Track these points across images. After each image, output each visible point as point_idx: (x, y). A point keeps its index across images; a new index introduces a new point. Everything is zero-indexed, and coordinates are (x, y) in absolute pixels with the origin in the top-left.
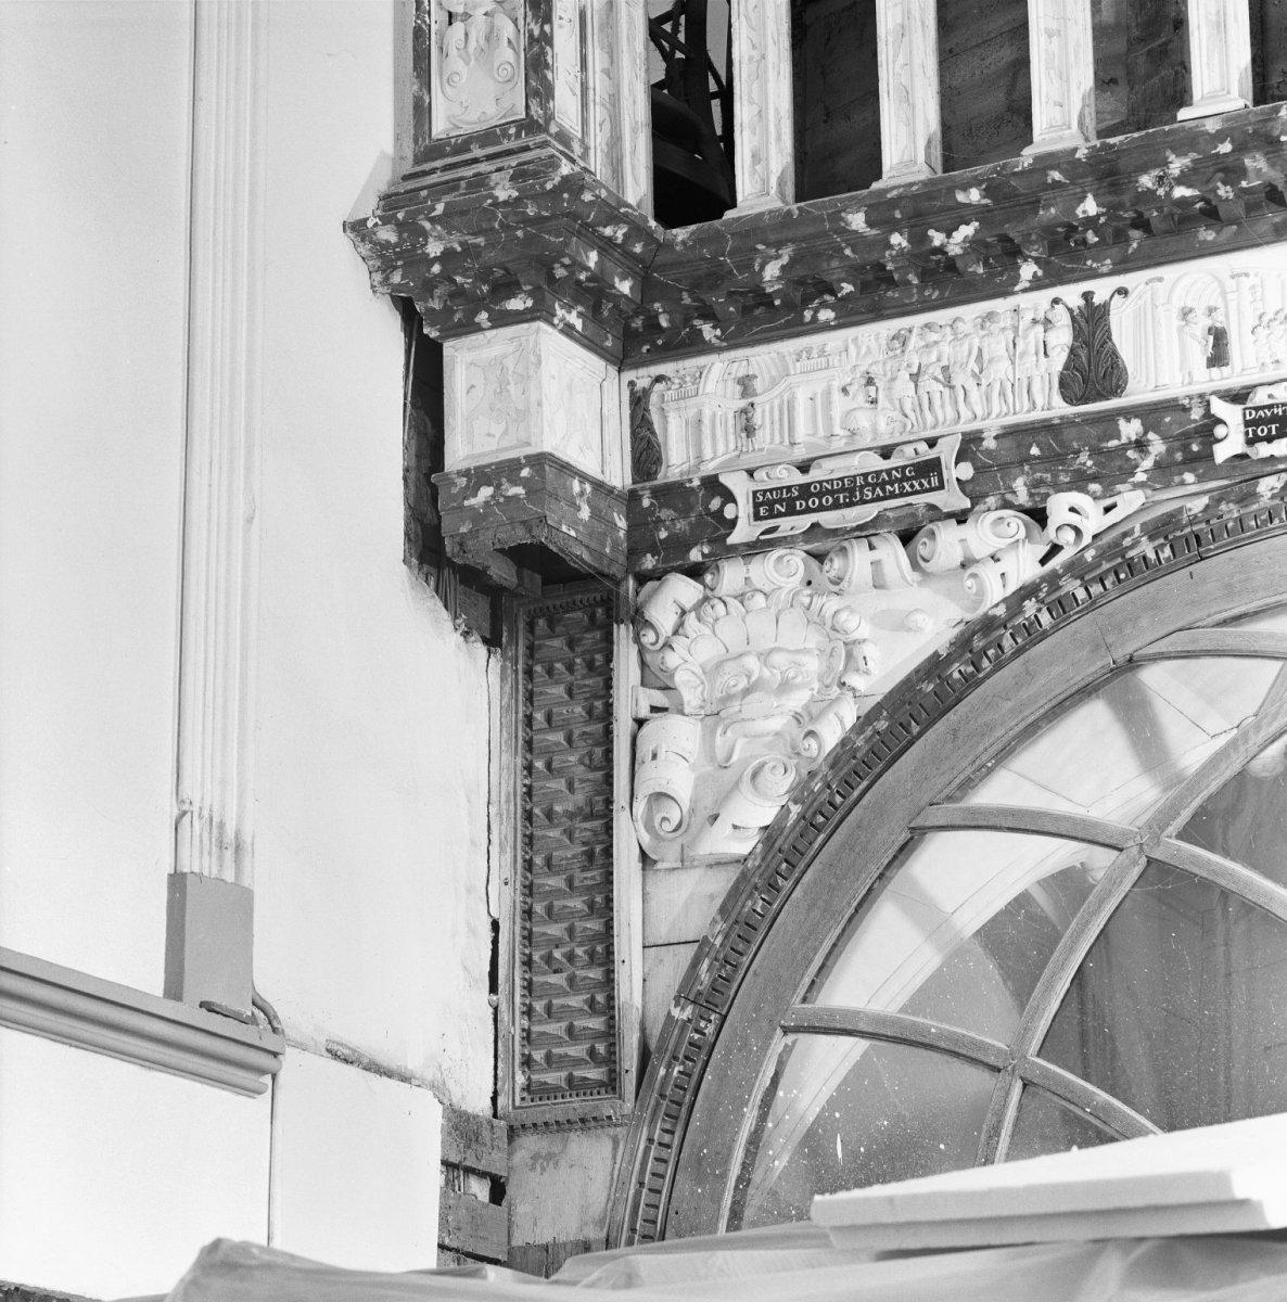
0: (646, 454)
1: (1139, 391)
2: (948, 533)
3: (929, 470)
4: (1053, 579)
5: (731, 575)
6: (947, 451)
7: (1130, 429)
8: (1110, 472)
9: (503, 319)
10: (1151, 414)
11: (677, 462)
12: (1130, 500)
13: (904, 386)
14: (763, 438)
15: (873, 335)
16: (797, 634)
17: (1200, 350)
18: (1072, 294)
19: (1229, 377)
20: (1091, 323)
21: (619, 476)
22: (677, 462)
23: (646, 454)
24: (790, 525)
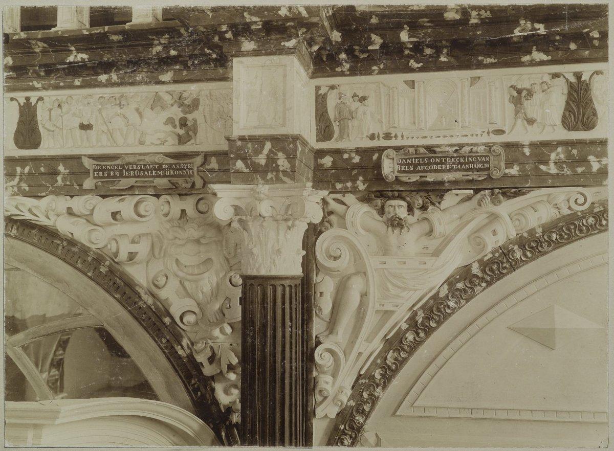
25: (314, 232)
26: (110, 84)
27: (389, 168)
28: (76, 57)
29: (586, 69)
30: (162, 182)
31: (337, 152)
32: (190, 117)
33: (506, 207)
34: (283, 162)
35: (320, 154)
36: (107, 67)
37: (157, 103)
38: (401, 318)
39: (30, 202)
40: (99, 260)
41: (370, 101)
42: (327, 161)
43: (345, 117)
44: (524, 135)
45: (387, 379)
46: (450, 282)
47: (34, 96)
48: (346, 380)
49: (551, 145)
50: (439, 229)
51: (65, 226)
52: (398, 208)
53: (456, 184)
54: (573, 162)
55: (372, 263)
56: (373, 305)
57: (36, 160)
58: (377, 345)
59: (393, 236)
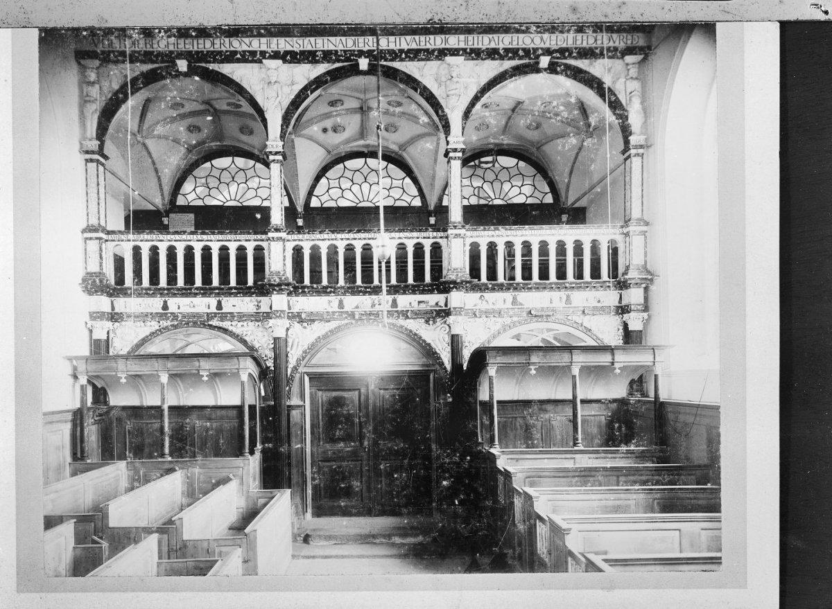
0: (113, 308)
1: (170, 311)
4: (160, 329)
5: (123, 323)
7: (170, 315)
9: (97, 295)
10: (171, 313)
12: (168, 321)
18: (163, 299)
19: (179, 311)
20: (165, 302)
21: (110, 311)
23: (113, 308)
25: (288, 329)
27: (303, 316)
28: (233, 291)
35: (289, 313)
36: (240, 293)
38: (306, 347)
39: (221, 323)
40: (238, 336)
42: (290, 315)
44: (330, 310)
45: (303, 360)
47: (221, 299)
48: (295, 360)
51: (230, 328)
52: (305, 324)
56: (300, 344)
58: (301, 352)
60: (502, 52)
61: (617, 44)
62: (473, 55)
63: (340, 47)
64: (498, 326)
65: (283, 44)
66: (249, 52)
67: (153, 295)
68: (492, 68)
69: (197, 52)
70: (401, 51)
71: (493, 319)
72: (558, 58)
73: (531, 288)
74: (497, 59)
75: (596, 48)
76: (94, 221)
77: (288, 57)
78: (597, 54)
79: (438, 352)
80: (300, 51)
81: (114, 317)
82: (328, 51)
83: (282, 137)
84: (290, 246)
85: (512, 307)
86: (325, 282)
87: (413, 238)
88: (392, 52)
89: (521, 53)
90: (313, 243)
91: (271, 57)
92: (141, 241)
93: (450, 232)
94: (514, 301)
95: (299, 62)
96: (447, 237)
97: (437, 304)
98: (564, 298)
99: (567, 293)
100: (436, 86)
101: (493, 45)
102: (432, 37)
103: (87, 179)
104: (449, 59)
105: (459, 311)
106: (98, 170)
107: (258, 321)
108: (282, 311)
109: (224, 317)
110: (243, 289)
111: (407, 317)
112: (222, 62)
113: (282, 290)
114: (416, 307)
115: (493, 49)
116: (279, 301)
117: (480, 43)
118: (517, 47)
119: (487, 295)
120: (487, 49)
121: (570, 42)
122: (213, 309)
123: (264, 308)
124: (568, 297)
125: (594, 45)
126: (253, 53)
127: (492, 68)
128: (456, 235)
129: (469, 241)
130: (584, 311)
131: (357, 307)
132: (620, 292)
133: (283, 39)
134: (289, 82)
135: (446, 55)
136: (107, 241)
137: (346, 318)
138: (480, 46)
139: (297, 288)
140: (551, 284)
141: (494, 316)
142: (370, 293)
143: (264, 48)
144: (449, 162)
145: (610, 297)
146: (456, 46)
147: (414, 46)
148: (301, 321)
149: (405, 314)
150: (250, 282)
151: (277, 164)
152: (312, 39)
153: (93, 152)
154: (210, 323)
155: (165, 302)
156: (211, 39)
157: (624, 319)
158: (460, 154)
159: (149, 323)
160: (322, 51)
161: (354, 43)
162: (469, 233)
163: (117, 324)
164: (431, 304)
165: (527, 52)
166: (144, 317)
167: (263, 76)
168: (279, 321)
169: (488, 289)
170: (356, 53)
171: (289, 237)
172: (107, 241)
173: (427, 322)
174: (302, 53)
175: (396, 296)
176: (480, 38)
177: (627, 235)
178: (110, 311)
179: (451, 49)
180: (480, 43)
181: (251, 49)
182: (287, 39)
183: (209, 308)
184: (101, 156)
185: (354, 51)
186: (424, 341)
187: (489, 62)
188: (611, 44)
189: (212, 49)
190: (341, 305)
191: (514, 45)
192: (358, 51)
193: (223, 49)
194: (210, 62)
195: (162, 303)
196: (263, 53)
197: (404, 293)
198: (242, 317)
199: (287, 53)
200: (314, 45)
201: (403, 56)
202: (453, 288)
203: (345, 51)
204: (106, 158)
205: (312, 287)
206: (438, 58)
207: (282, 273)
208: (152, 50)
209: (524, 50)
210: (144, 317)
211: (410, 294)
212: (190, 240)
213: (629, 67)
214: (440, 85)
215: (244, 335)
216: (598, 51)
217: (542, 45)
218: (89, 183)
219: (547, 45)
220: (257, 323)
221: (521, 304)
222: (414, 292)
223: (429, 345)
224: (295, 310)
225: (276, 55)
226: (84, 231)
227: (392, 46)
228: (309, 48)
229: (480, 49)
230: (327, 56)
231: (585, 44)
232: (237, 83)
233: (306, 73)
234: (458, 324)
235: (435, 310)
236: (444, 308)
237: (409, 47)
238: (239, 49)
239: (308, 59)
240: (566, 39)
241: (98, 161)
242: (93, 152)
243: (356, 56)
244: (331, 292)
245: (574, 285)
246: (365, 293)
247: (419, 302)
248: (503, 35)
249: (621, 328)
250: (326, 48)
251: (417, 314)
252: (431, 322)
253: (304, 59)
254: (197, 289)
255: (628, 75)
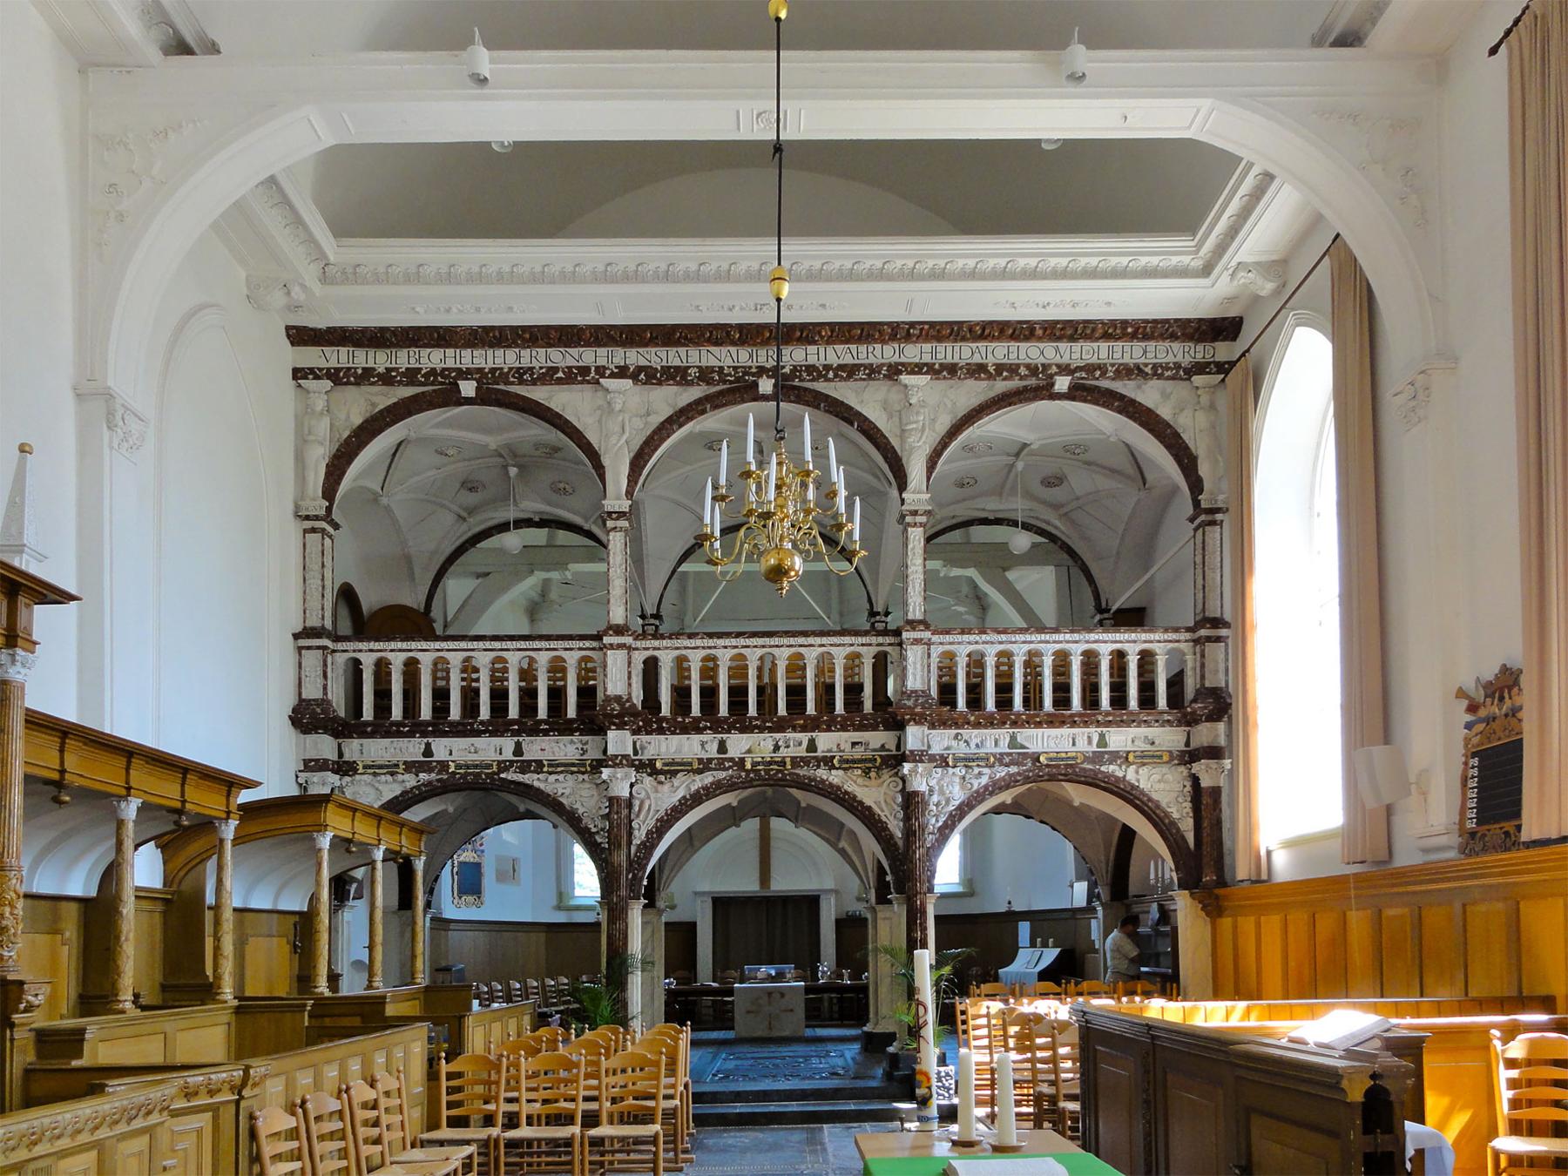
0: (341, 755)
2: (400, 776)
3: (397, 766)
5: (357, 777)
6: (401, 764)
7: (435, 764)
8: (430, 771)
11: (347, 757)
12: (433, 775)
13: (392, 750)
14: (365, 754)
15: (387, 741)
16: (369, 790)
17: (448, 753)
18: (425, 740)
20: (428, 745)
21: (336, 758)
22: (347, 757)
23: (341, 755)
24: (369, 771)
26: (554, 735)
27: (659, 765)
29: (725, 736)
30: (575, 769)
31: (640, 760)
32: (585, 747)
33: (698, 777)
34: (624, 762)
36: (553, 730)
37: (572, 742)
38: (662, 813)
41: (653, 744)
43: (643, 748)
44: (705, 756)
46: (680, 801)
47: (521, 739)
49: (713, 759)
50: (676, 784)
51: (536, 784)
52: (662, 778)
53: (682, 771)
54: (720, 764)
55: (652, 796)
57: (523, 761)
59: (660, 787)
60: (991, 369)
61: (1179, 358)
62: (945, 373)
63: (729, 362)
64: (984, 780)
65: (634, 357)
66: (578, 368)
67: (410, 734)
68: (972, 392)
69: (493, 370)
70: (827, 367)
71: (976, 770)
72: (1083, 378)
73: (1040, 723)
74: (983, 380)
75: (1146, 365)
76: (314, 622)
77: (642, 376)
78: (1147, 374)
79: (884, 819)
80: (662, 367)
81: (344, 768)
82: (707, 367)
83: (629, 493)
84: (639, 658)
85: (1008, 751)
86: (696, 710)
87: (844, 645)
88: (811, 369)
89: (1023, 371)
90: (677, 652)
91: (612, 375)
92: (392, 651)
93: (905, 635)
94: (1013, 742)
95: (660, 383)
96: (900, 644)
97: (883, 746)
98: (1095, 739)
99: (1099, 730)
100: (884, 417)
101: (977, 359)
102: (877, 347)
103: (304, 557)
104: (905, 378)
105: (918, 757)
106: (323, 545)
107: (583, 773)
108: (625, 756)
109: (525, 767)
110: (558, 724)
111: (833, 767)
112: (534, 382)
113: (625, 724)
114: (849, 753)
115: (977, 365)
116: (619, 741)
117: (957, 356)
118: (1017, 361)
119: (966, 733)
120: (967, 364)
121: (1104, 355)
122: (508, 754)
123: (594, 754)
124: (1102, 736)
125: (1143, 360)
126: (585, 370)
127: (972, 392)
128: (915, 640)
129: (936, 651)
130: (1127, 758)
131: (749, 751)
132: (1187, 729)
133: (634, 350)
134: (643, 411)
135: (900, 372)
136: (334, 651)
137: (730, 767)
138: (956, 360)
139: (646, 718)
140: (1072, 716)
141: (978, 765)
142: (771, 730)
143: (602, 362)
144: (905, 530)
145: (1170, 738)
146: (917, 360)
147: (848, 360)
148: (654, 772)
149: (828, 762)
150: (571, 712)
151: (618, 534)
152: (682, 350)
153: (317, 518)
154: (502, 776)
155: (428, 745)
156: (517, 350)
157: (1193, 771)
158: (923, 519)
159: (400, 777)
160: (698, 367)
161: (751, 356)
162: (935, 638)
163: (347, 779)
164: (871, 747)
165: (1033, 370)
166: (392, 769)
167: (600, 402)
168: (620, 772)
169: (968, 723)
170: (754, 370)
171: (639, 644)
172: (334, 651)
173: (866, 772)
174: (666, 369)
175: (814, 734)
176: (957, 349)
177: (1196, 641)
178: (336, 758)
179: (910, 364)
180: (957, 356)
181: (581, 364)
182: (640, 350)
183: (501, 754)
184: (328, 523)
185: (750, 367)
186: (861, 803)
187: (971, 382)
188: (1170, 359)
189: (517, 365)
190: (722, 748)
191: (1013, 359)
192: (757, 367)
193: (535, 364)
194: (513, 383)
195: (423, 746)
196: (601, 371)
197: (829, 730)
198: (555, 767)
199: (640, 369)
200: (685, 361)
201: (831, 375)
202: (909, 721)
203: (735, 368)
204: (336, 526)
205: (675, 720)
206: (888, 377)
207: (625, 697)
208: (417, 366)
209: (1028, 366)
210: (392, 769)
211: (838, 730)
212: (473, 650)
213: (1199, 392)
214: (890, 417)
215: (560, 793)
216: (1148, 370)
217: (1058, 360)
218: (307, 564)
219: (1066, 360)
220: (581, 777)
221: (1023, 747)
222: (844, 729)
223: (869, 808)
224: (645, 756)
225: (622, 372)
226: (296, 636)
227: (812, 360)
228: (677, 362)
229: (956, 364)
230: (705, 375)
231: (1127, 360)
232: (557, 413)
233: (667, 399)
234: (921, 779)
235: (880, 756)
236: (894, 753)
237: (841, 362)
238: (563, 365)
239: (673, 379)
240: (1096, 350)
241: (323, 531)
242: (317, 518)
243: (753, 375)
244: (706, 728)
245: (1110, 718)
246: (761, 729)
247: (854, 744)
248: (994, 345)
249: (1188, 784)
250: (704, 363)
251: (848, 764)
252: (873, 774)
253: (667, 379)
254: (482, 723)
255: (1199, 402)
